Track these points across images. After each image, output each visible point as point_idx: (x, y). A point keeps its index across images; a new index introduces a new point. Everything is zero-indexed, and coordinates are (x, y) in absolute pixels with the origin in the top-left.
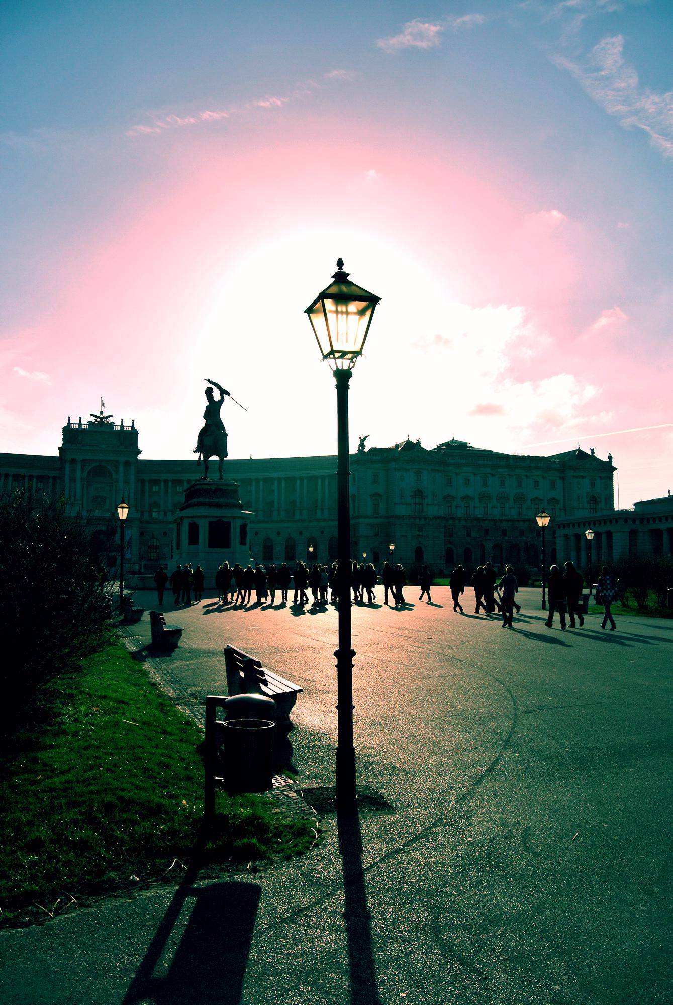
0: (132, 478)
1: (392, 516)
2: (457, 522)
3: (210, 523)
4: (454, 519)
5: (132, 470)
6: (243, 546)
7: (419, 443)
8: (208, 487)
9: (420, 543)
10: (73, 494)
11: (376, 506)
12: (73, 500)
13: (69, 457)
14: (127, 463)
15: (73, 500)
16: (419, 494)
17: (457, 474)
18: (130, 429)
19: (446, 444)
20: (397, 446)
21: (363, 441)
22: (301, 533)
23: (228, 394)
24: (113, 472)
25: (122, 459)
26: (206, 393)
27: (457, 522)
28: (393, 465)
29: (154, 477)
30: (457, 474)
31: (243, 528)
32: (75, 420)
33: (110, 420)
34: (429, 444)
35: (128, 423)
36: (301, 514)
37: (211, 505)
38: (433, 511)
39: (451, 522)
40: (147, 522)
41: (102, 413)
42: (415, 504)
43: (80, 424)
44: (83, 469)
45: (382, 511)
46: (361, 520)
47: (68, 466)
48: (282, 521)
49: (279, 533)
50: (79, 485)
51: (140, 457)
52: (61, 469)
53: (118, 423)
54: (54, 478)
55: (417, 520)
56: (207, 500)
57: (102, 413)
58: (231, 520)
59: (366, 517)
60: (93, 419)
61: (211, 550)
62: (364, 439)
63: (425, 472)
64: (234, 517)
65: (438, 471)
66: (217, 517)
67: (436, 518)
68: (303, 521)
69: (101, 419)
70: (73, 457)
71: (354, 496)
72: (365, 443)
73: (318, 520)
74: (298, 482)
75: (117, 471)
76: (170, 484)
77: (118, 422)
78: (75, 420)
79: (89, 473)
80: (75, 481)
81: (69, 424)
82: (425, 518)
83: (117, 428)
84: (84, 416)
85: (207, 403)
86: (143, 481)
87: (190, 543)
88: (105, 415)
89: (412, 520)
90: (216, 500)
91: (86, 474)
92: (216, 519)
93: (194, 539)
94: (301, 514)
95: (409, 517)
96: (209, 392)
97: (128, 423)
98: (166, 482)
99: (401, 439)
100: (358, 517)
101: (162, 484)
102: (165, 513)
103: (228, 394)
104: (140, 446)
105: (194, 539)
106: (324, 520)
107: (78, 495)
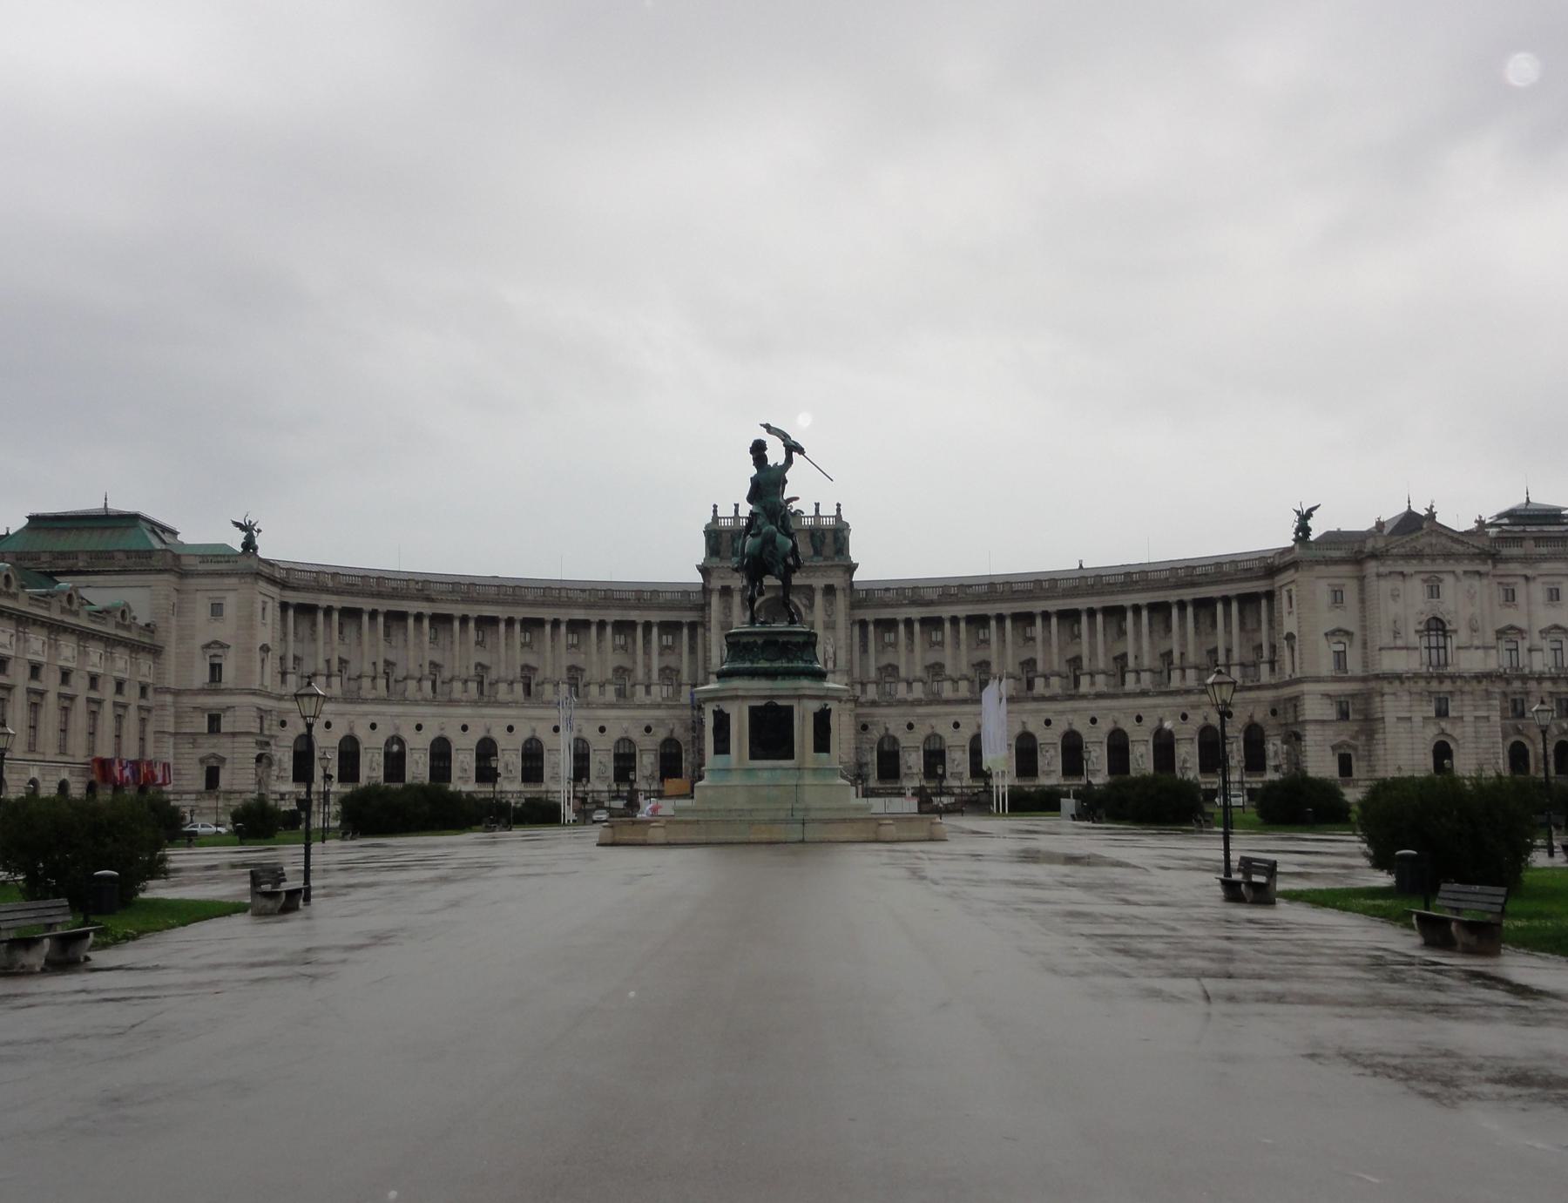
0: (841, 619)
1: (1377, 677)
2: (1532, 685)
3: (753, 710)
4: (1524, 679)
5: (841, 602)
7: (1431, 515)
8: (751, 639)
9: (1443, 732)
11: (1340, 658)
13: (716, 584)
14: (829, 590)
16: (1437, 626)
17: (1527, 578)
18: (832, 521)
19: (1510, 514)
20: (1380, 525)
21: (1304, 517)
23: (801, 451)
24: (803, 609)
26: (753, 451)
27: (1532, 685)
28: (1372, 567)
29: (886, 614)
30: (1527, 578)
32: (726, 511)
33: (795, 506)
34: (1458, 517)
35: (828, 510)
36: (1183, 677)
37: (753, 674)
38: (1470, 662)
39: (1517, 685)
40: (874, 704)
42: (1429, 648)
45: (1354, 666)
46: (1306, 687)
47: (715, 600)
48: (1144, 694)
49: (1139, 719)
51: (856, 577)
52: (703, 607)
53: (809, 511)
54: (693, 626)
56: (748, 665)
58: (794, 703)
59: (1318, 680)
62: (1309, 514)
63: (1449, 580)
65: (1478, 573)
67: (1479, 677)
68: (1188, 692)
70: (726, 583)
71: (1290, 637)
72: (1310, 523)
74: (1175, 612)
75: (811, 606)
76: (917, 627)
77: (809, 511)
78: (726, 511)
81: (716, 518)
82: (1453, 678)
83: (807, 522)
86: (863, 624)
87: (717, 752)
89: (1422, 684)
90: (763, 664)
92: (761, 703)
94: (1183, 677)
95: (1416, 676)
96: (758, 449)
97: (828, 510)
98: (909, 623)
99: (1392, 510)
100: (1299, 681)
101: (902, 628)
102: (909, 684)
103: (801, 451)
104: (855, 554)
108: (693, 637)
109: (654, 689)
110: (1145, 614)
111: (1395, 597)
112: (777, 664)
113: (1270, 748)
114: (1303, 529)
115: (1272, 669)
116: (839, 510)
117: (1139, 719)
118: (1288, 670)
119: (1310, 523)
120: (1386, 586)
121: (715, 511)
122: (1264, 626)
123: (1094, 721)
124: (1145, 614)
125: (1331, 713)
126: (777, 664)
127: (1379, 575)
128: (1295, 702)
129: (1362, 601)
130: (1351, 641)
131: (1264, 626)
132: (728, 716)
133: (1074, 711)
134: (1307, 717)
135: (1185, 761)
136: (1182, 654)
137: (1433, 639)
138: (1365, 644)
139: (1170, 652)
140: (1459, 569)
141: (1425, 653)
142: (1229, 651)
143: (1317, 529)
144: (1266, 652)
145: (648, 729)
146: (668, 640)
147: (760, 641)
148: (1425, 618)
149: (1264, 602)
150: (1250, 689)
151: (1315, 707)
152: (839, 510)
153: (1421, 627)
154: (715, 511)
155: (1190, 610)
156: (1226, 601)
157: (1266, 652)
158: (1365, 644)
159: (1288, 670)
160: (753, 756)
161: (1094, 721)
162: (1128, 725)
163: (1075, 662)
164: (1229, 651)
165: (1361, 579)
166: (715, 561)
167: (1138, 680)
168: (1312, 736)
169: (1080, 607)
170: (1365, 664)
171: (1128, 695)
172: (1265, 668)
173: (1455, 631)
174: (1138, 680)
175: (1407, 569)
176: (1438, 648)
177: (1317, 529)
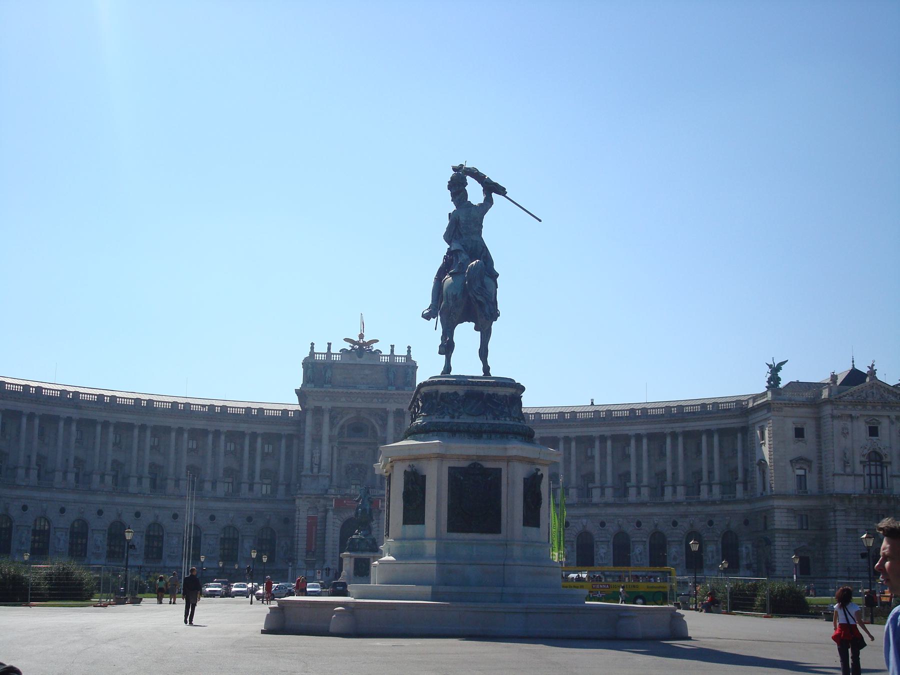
6: (532, 531)
7: (872, 372)
10: (316, 460)
11: (801, 480)
12: (316, 470)
13: (311, 404)
15: (316, 470)
16: (876, 458)
21: (775, 370)
22: (675, 524)
23: (502, 191)
24: (377, 427)
25: (392, 407)
31: (532, 485)
32: (320, 348)
33: (375, 347)
35: (401, 351)
41: (361, 336)
42: (870, 475)
43: (329, 353)
44: (332, 425)
45: (812, 485)
46: (776, 503)
47: (309, 419)
48: (643, 504)
49: (639, 524)
50: (326, 447)
53: (386, 351)
54: (290, 438)
55: (875, 503)
56: (447, 419)
57: (361, 336)
59: (784, 496)
60: (348, 346)
61: (455, 535)
63: (885, 423)
64: (509, 459)
66: (468, 458)
68: (678, 503)
69: (361, 345)
70: (317, 404)
72: (780, 374)
73: (704, 503)
75: (384, 426)
77: (386, 351)
78: (320, 348)
79: (342, 427)
80: (320, 441)
81: (312, 353)
83: (384, 359)
84: (334, 339)
85: (452, 208)
87: (407, 521)
88: (366, 339)
90: (465, 419)
91: (336, 431)
93: (414, 511)
96: (457, 186)
97: (401, 351)
100: (771, 497)
103: (502, 191)
105: (414, 511)
106: (714, 503)
107: (324, 464)
108: (289, 447)
109: (256, 487)
110: (645, 441)
111: (845, 434)
112: (481, 420)
113: (743, 550)
114: (774, 380)
115: (745, 489)
116: (409, 351)
117: (639, 524)
118: (759, 489)
119: (780, 374)
120: (838, 425)
121: (312, 348)
122: (740, 455)
123: (603, 524)
124: (645, 441)
125: (794, 524)
126: (481, 420)
127: (833, 417)
128: (766, 515)
129: (819, 436)
130: (810, 466)
131: (740, 455)
132: (424, 477)
133: (587, 516)
134: (776, 527)
135: (675, 559)
136: (673, 474)
137: (873, 468)
138: (820, 471)
139: (665, 472)
140: (893, 415)
141: (867, 478)
142: (711, 472)
143: (786, 377)
144: (740, 475)
145: (250, 519)
146: (268, 448)
147: (461, 393)
148: (866, 452)
149: (739, 435)
150: (728, 503)
151: (781, 520)
152: (409, 351)
153: (864, 459)
154: (312, 348)
155: (680, 440)
156: (710, 433)
157: (740, 475)
158: (820, 471)
159: (759, 489)
160: (453, 527)
161: (603, 524)
162: (630, 529)
163: (588, 478)
164: (711, 472)
165: (818, 420)
166: (310, 386)
167: (639, 493)
168: (779, 542)
169: (594, 434)
170: (820, 486)
171: (630, 504)
172: (739, 488)
173: (890, 463)
174: (639, 493)
175: (854, 413)
176: (876, 475)
177: (786, 377)
